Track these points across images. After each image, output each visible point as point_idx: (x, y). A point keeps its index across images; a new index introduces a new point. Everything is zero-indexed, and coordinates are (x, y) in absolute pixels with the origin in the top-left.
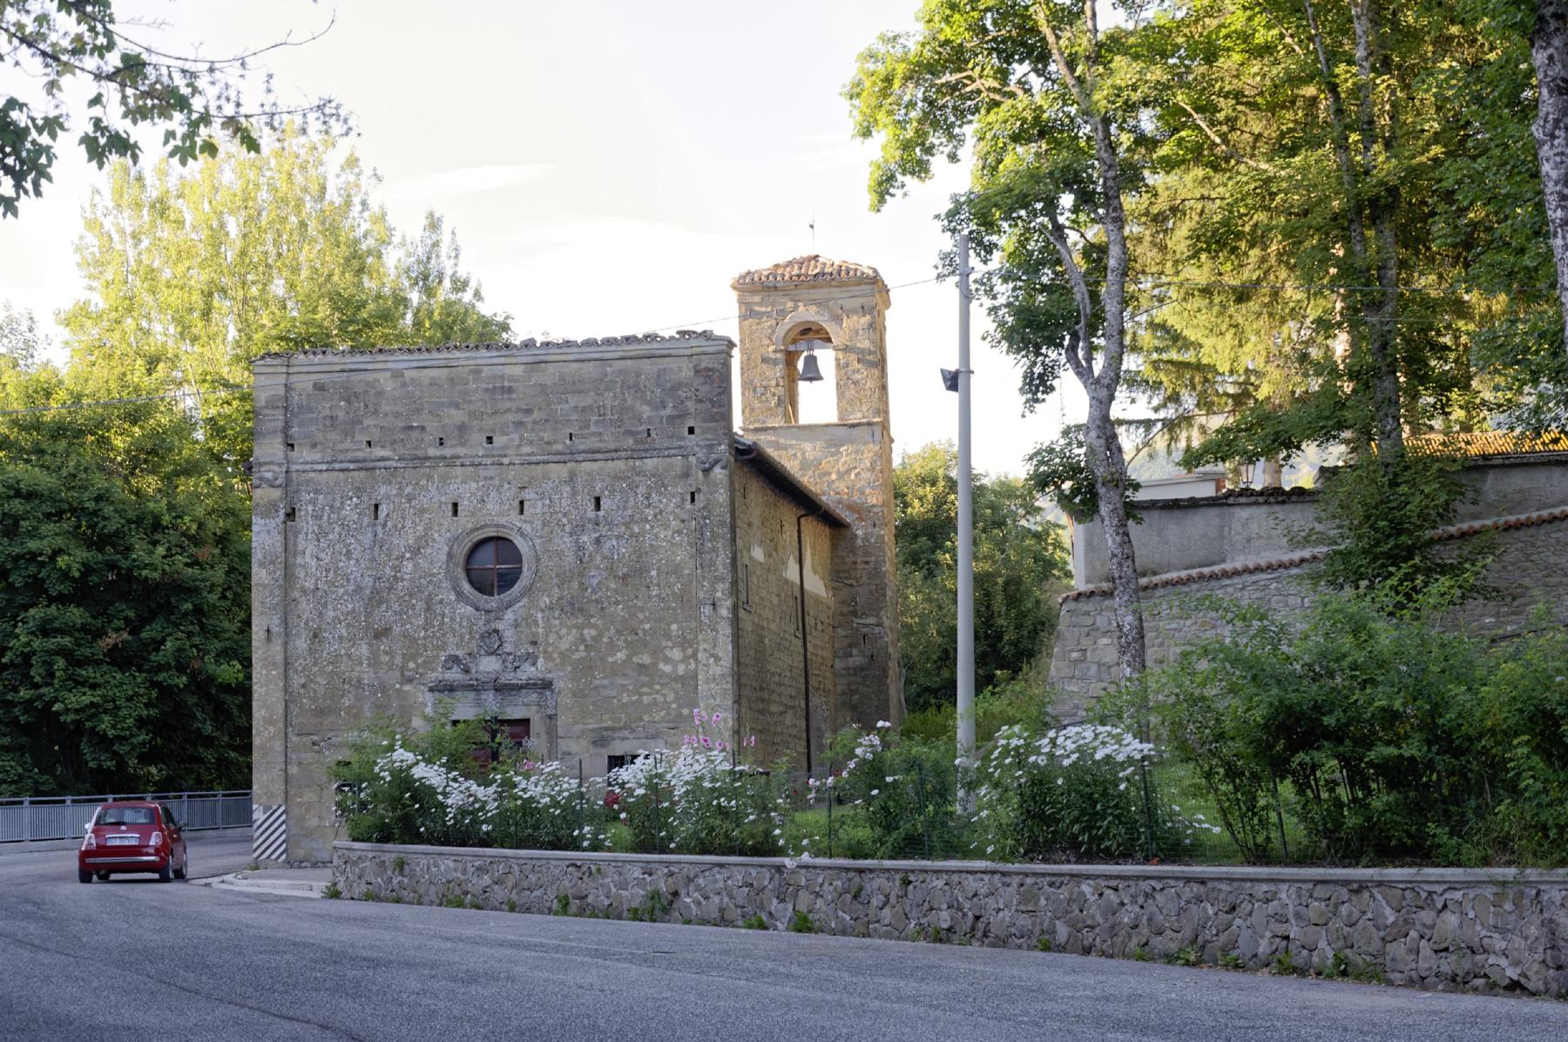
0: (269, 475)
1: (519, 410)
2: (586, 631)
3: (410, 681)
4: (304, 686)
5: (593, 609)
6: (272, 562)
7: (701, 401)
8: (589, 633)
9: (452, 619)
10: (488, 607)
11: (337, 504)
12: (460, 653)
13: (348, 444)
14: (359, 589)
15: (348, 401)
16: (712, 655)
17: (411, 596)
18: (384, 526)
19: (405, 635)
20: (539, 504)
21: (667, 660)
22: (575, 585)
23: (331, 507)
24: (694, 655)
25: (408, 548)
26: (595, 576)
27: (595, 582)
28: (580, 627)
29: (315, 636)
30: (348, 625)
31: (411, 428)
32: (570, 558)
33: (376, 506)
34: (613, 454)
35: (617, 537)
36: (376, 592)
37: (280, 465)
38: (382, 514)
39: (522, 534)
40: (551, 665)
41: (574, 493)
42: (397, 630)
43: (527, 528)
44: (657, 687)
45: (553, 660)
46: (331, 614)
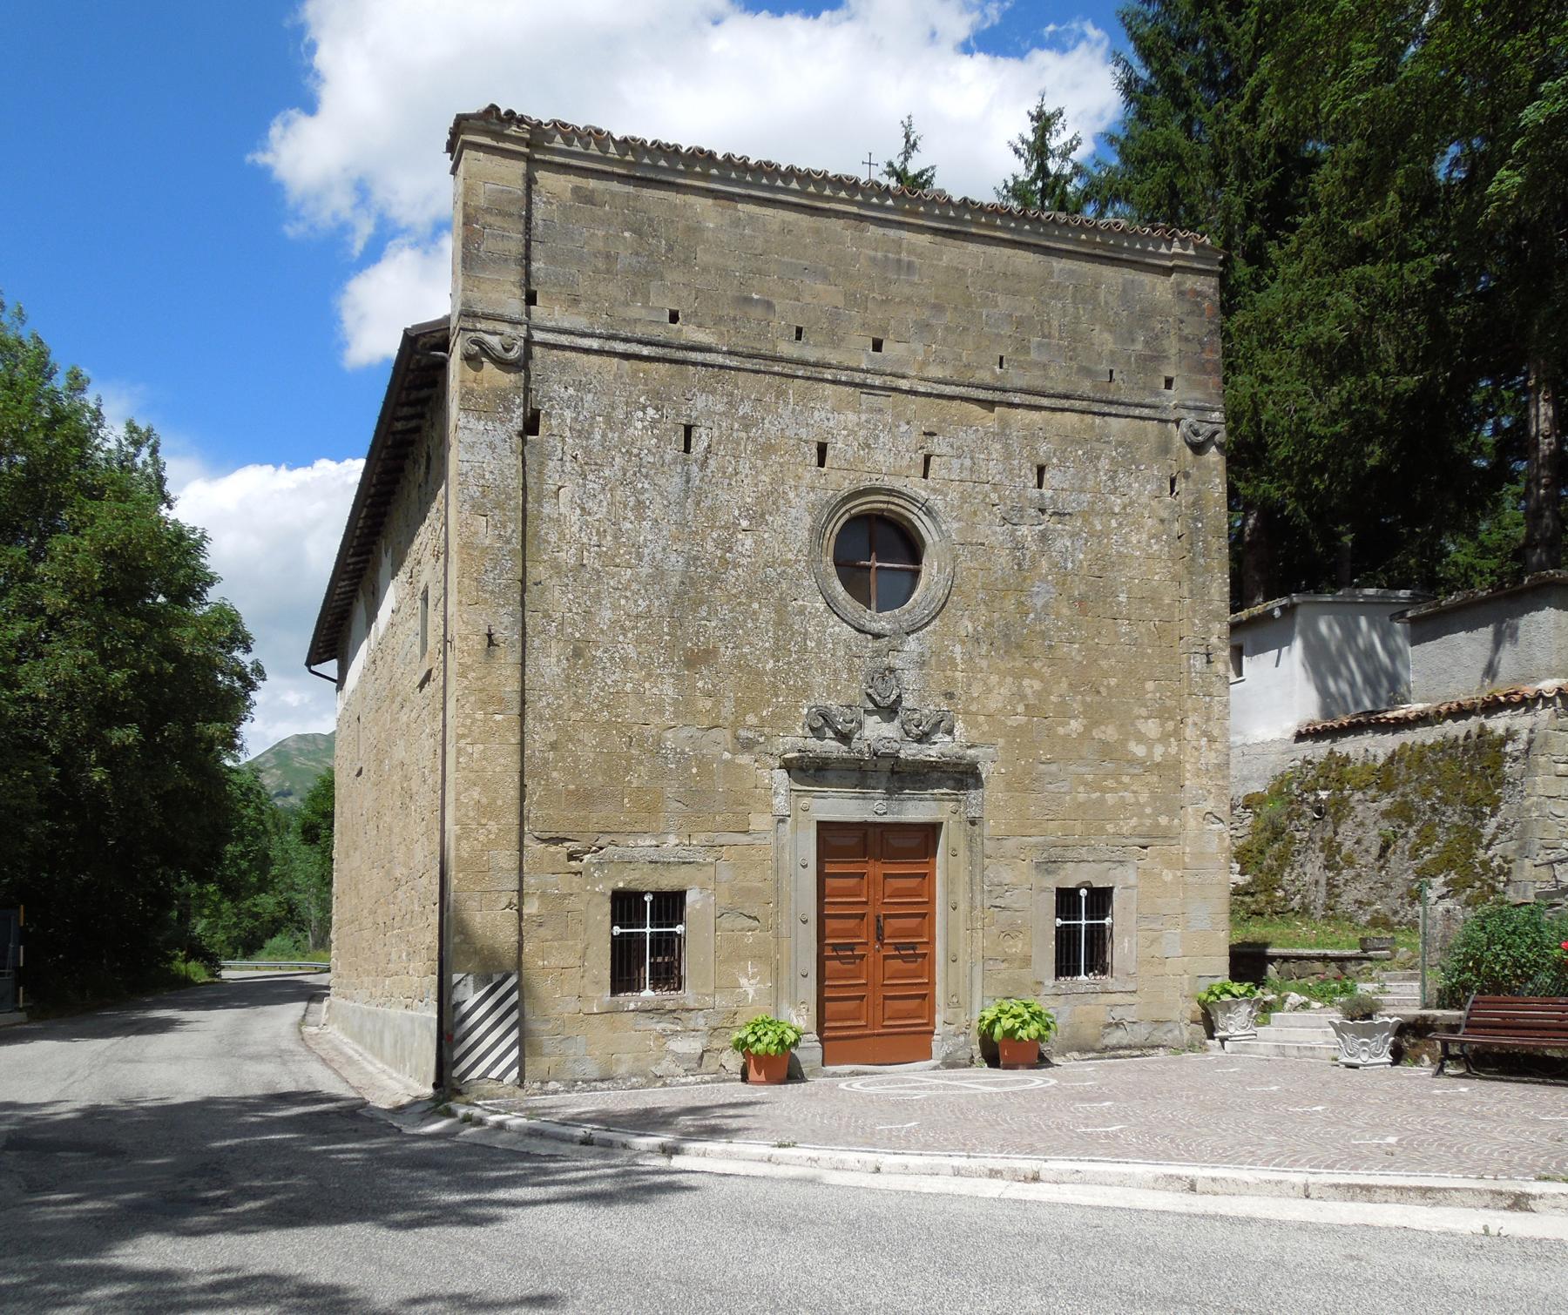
0: (494, 341)
1: (923, 302)
2: (1026, 682)
3: (747, 746)
4: (553, 746)
5: (1036, 646)
6: (499, 505)
7: (1186, 339)
8: (1031, 685)
9: (819, 642)
10: (876, 627)
11: (620, 414)
12: (833, 704)
13: (636, 311)
14: (659, 574)
15: (637, 231)
16: (1205, 733)
17: (750, 596)
18: (704, 465)
19: (741, 665)
20: (956, 463)
21: (1141, 738)
22: (1010, 604)
23: (608, 419)
24: (1177, 733)
25: (746, 511)
26: (1041, 594)
27: (1039, 602)
28: (1018, 676)
29: (577, 653)
30: (639, 640)
31: (748, 300)
32: (1003, 559)
33: (688, 430)
34: (1064, 400)
35: (1074, 535)
36: (688, 581)
37: (514, 323)
38: (698, 447)
39: (929, 512)
40: (974, 733)
41: (1008, 456)
42: (726, 653)
43: (937, 502)
44: (1126, 779)
45: (976, 725)
46: (608, 614)
